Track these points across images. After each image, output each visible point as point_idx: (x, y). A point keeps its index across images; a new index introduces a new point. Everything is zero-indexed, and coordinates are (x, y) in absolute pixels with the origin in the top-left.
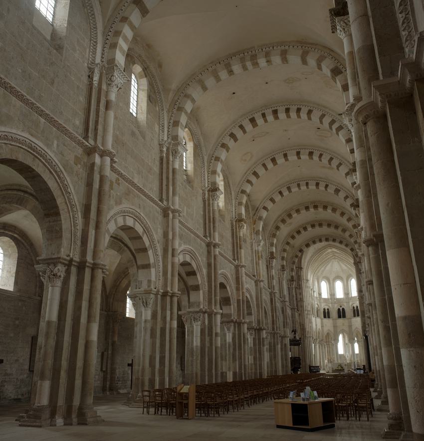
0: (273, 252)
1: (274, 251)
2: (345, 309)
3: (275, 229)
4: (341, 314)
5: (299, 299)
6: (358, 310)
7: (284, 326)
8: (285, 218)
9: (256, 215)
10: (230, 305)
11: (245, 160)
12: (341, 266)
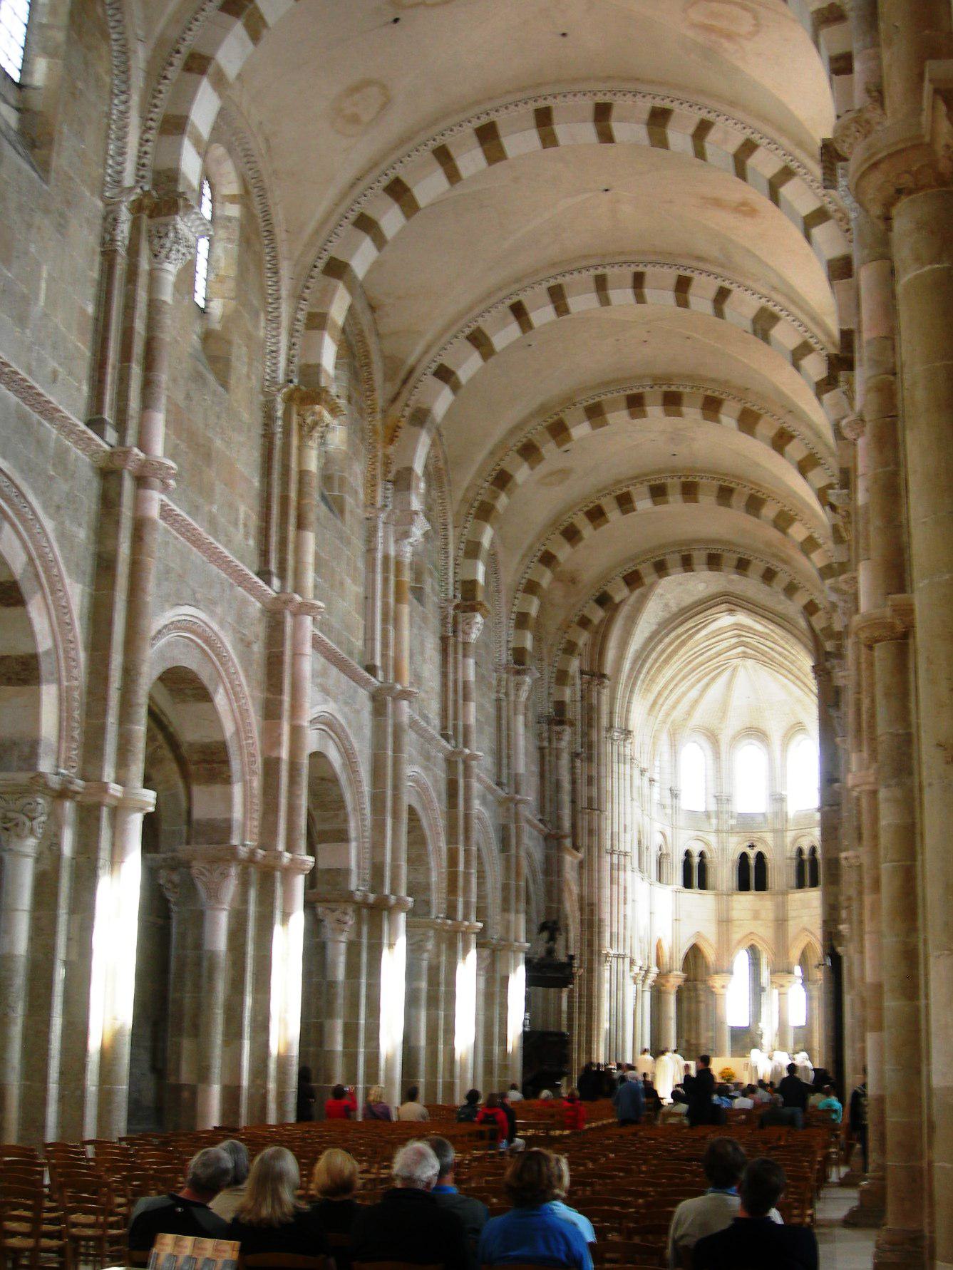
0: (474, 583)
1: (480, 578)
2: (768, 855)
3: (492, 484)
5: (582, 802)
6: (814, 861)
7: (506, 900)
8: (537, 440)
9: (400, 403)
10: (227, 781)
11: (355, 119)
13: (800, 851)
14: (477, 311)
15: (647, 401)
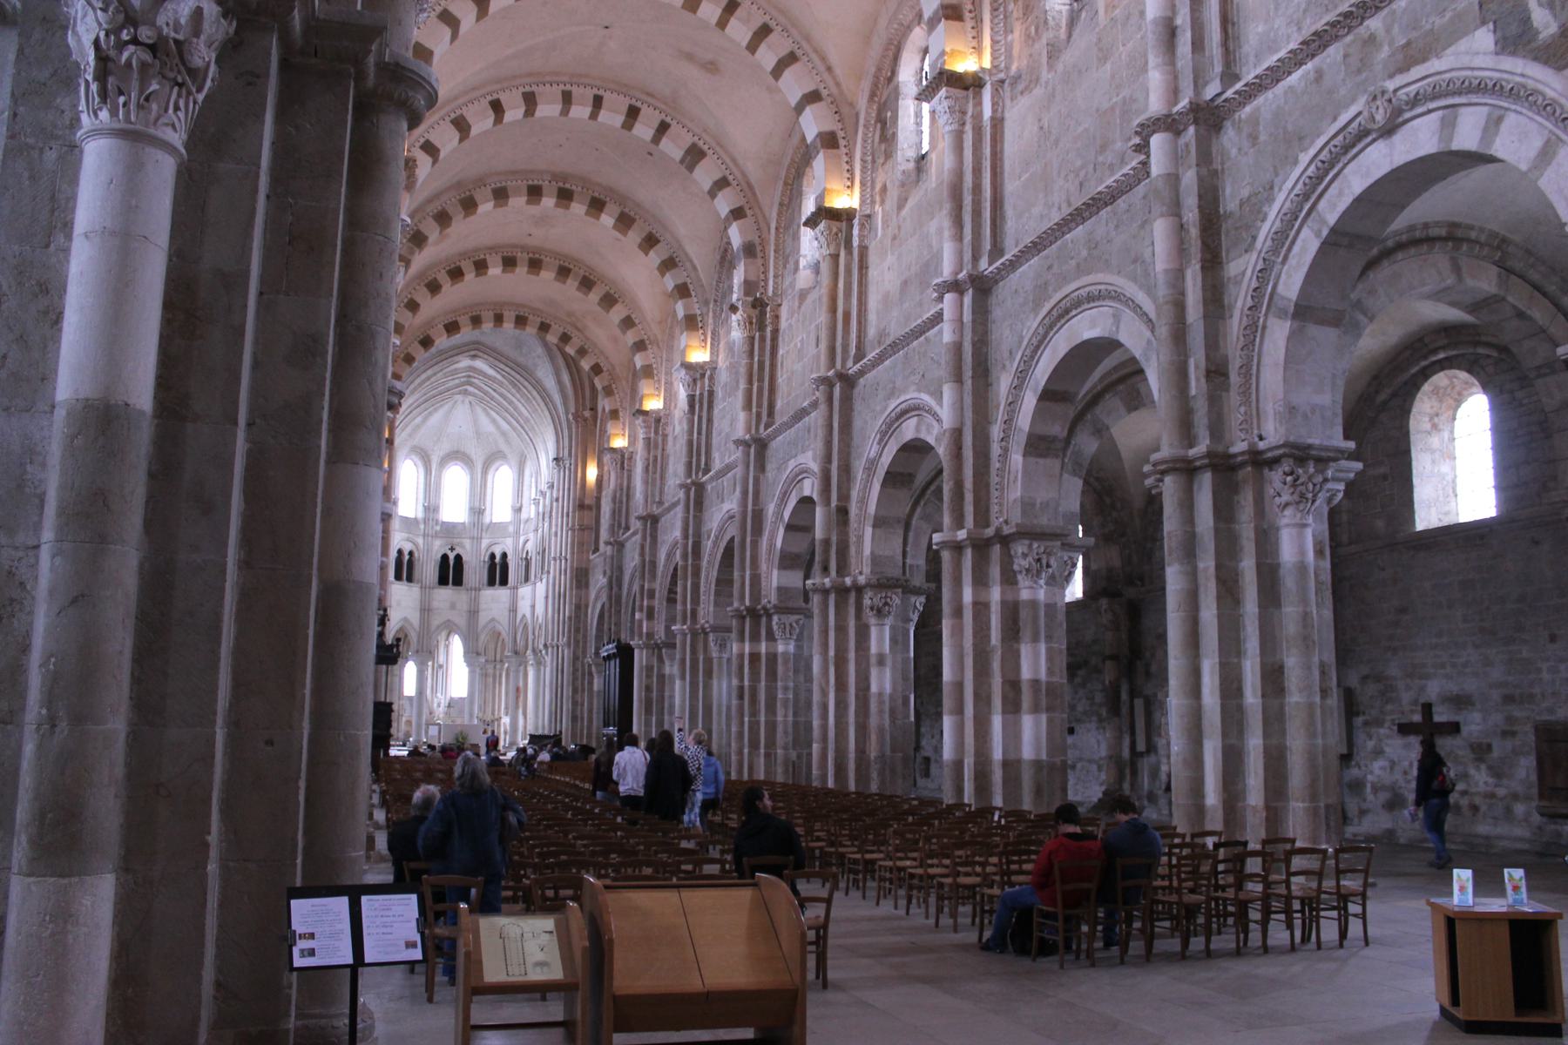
2: (464, 558)
4: (451, 572)
8: (450, 211)
12: (476, 422)
13: (493, 556)
14: (460, 101)
15: (544, 191)
